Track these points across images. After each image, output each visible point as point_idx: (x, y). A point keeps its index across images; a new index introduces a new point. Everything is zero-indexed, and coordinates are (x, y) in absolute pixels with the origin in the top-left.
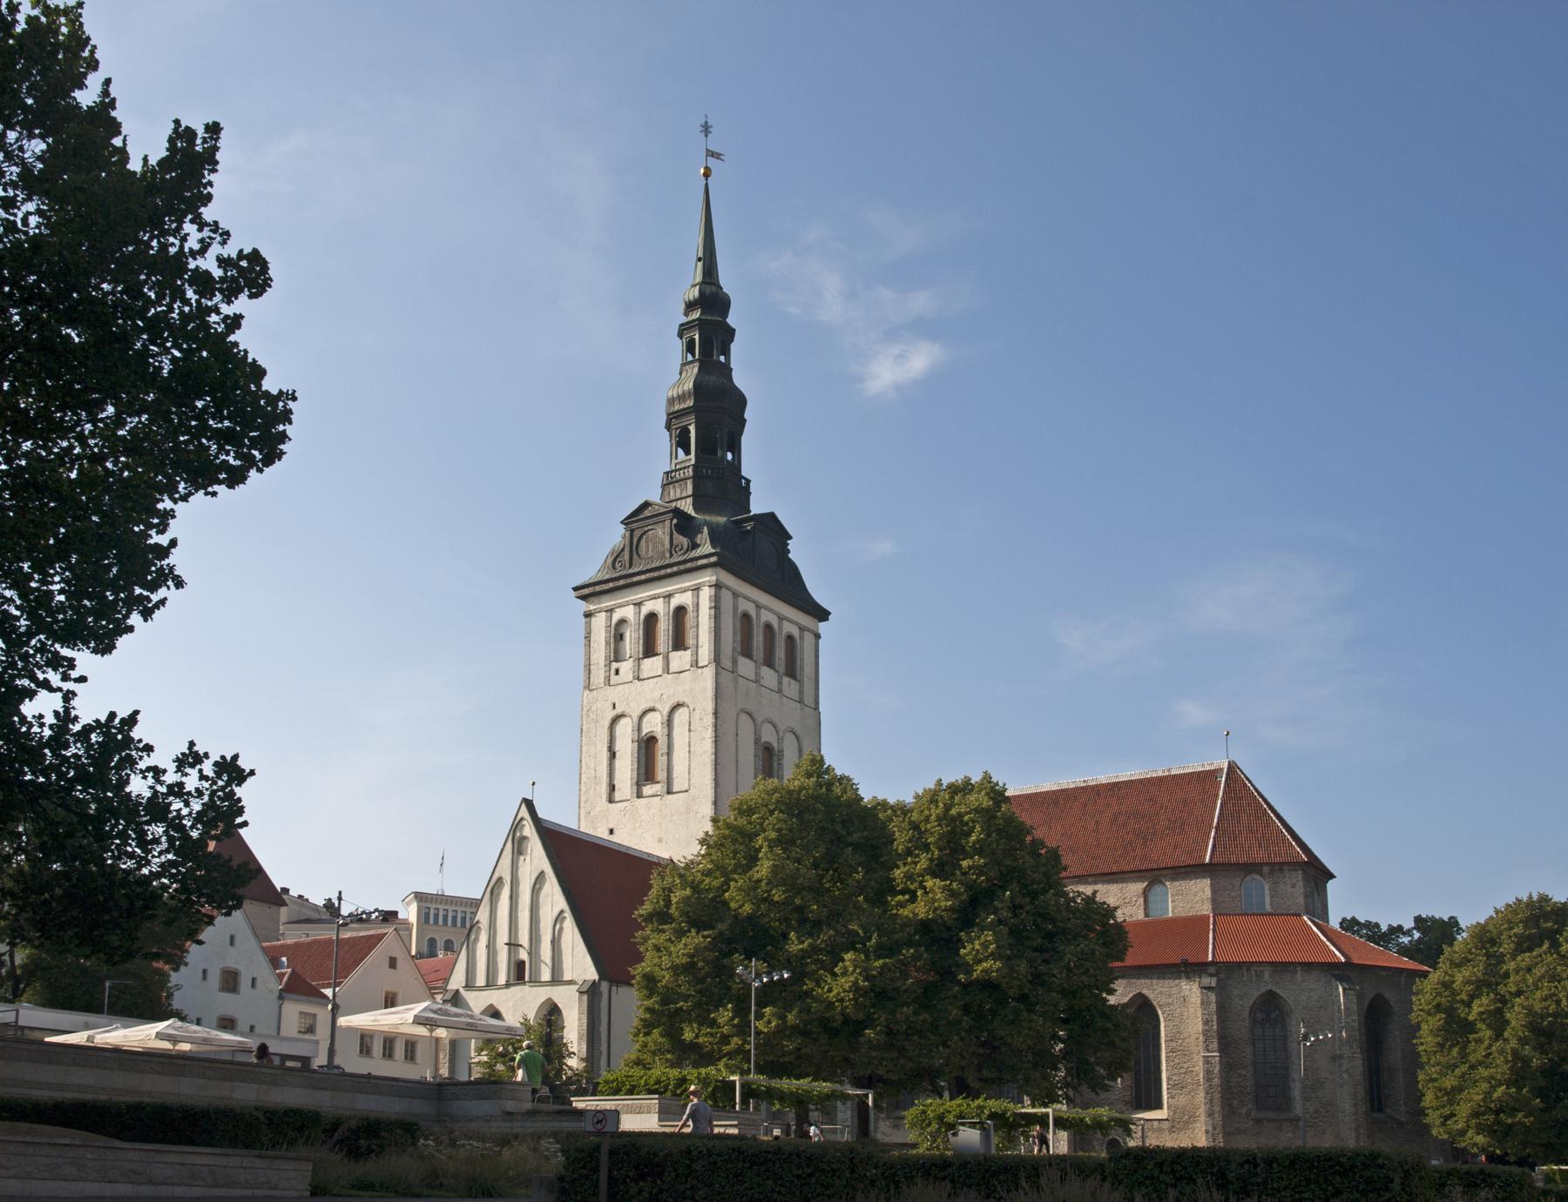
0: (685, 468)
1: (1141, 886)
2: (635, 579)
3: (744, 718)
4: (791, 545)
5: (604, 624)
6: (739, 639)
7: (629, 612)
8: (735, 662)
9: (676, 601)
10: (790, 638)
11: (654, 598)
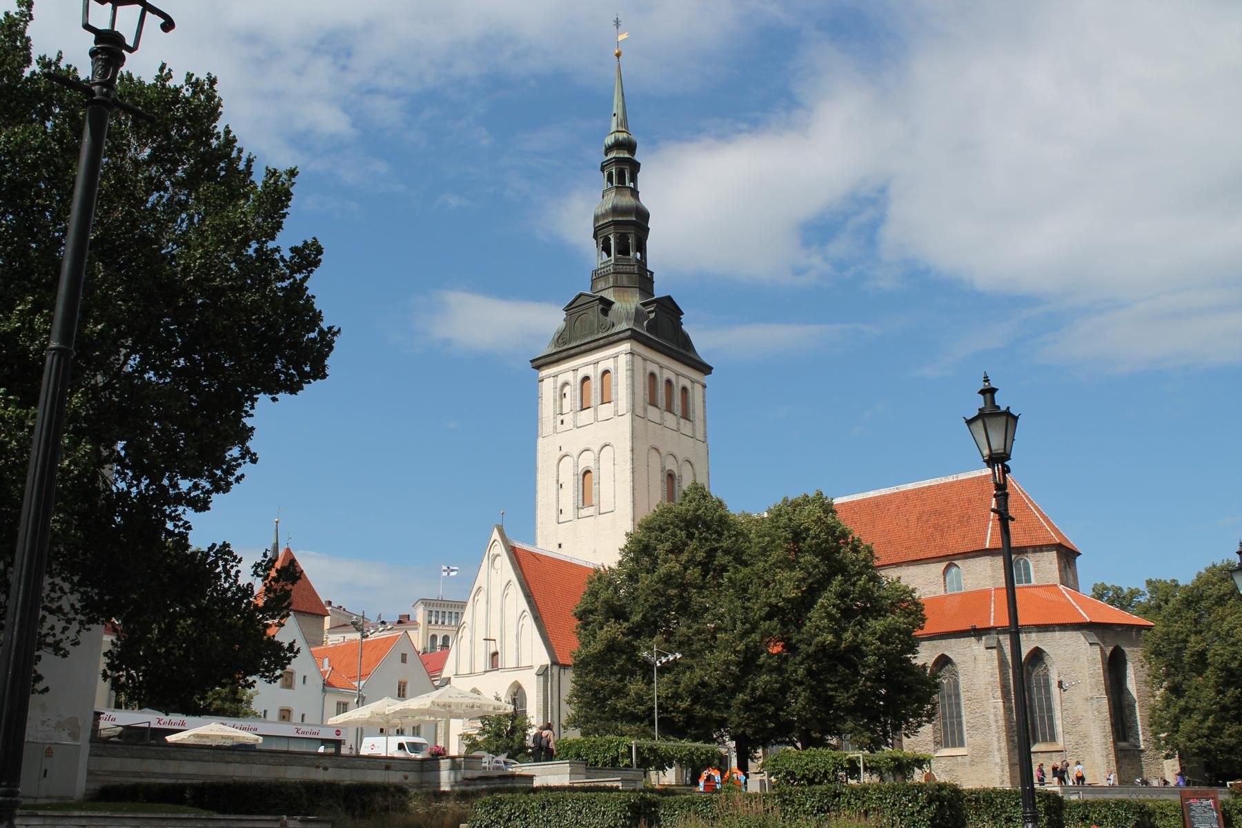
0: (607, 267)
1: (943, 565)
2: (573, 351)
3: (654, 453)
4: (684, 318)
5: (552, 386)
6: (647, 392)
7: (569, 376)
8: (645, 410)
9: (602, 366)
10: (684, 389)
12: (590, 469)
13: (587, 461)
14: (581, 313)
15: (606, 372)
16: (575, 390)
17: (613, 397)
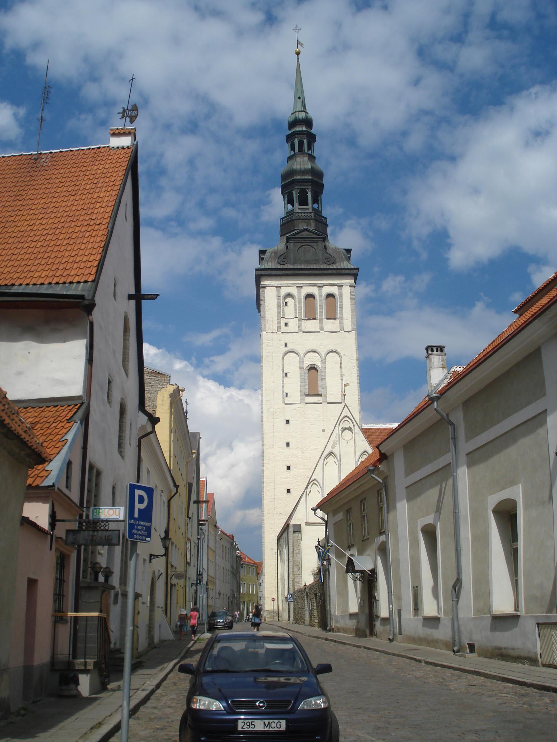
7: (294, 290)
9: (327, 290)
11: (312, 285)
12: (316, 367)
13: (312, 359)
14: (304, 244)
15: (330, 296)
16: (300, 302)
17: (339, 316)
